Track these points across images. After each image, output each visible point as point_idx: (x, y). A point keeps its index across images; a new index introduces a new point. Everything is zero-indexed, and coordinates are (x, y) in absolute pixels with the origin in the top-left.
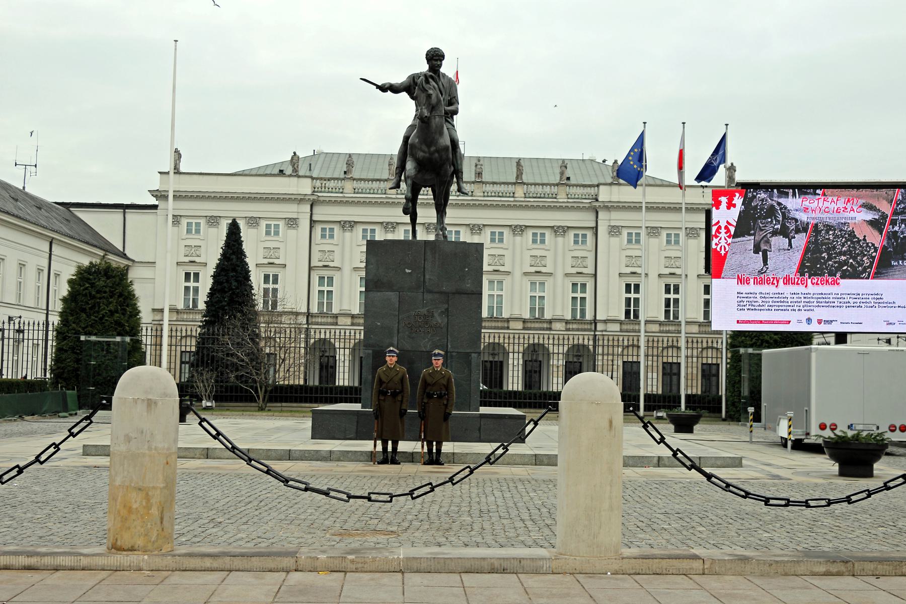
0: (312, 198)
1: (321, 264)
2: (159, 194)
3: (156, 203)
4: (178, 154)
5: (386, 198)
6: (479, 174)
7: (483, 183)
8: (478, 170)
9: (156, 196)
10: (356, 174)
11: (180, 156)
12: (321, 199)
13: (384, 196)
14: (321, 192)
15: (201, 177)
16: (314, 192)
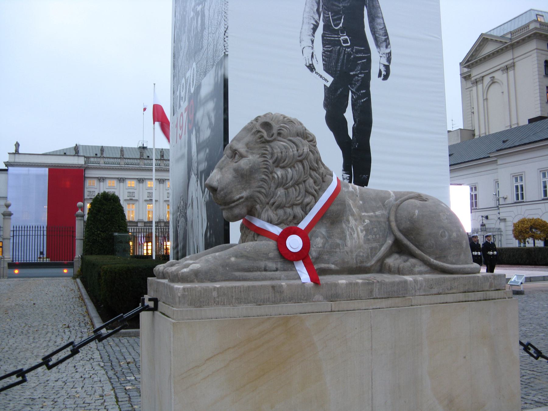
0: (85, 166)
1: (89, 197)
2: (9, 164)
3: (6, 168)
4: (17, 145)
5: (120, 166)
6: (162, 156)
7: (164, 160)
8: (162, 154)
9: (6, 166)
10: (105, 155)
11: (19, 145)
12: (90, 167)
13: (119, 165)
14: (89, 163)
15: (30, 155)
16: (85, 163)
